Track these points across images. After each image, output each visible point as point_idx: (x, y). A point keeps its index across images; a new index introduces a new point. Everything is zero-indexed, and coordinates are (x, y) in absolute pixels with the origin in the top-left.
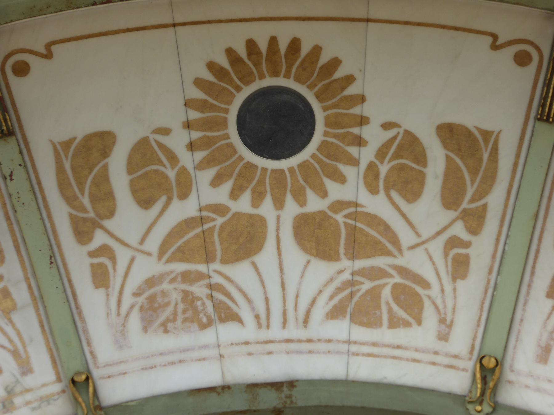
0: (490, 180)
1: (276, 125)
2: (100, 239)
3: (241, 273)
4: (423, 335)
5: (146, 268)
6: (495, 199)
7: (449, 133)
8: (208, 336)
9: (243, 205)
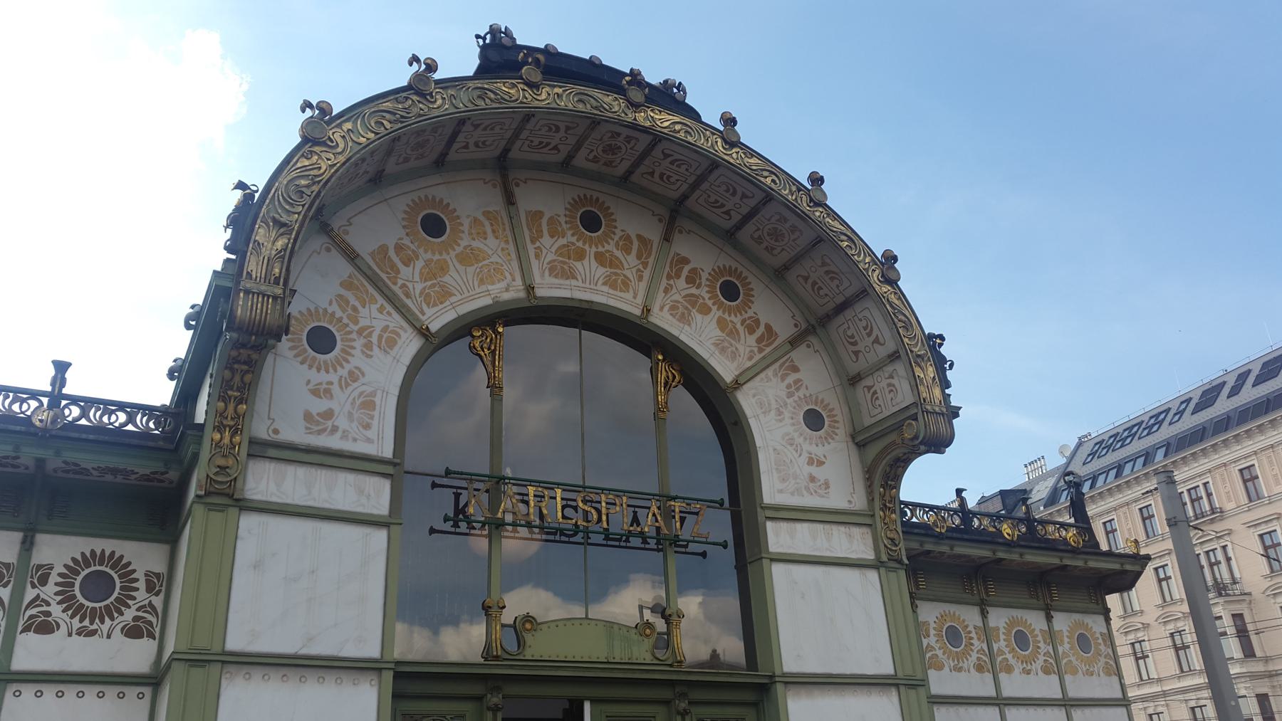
0: (649, 254)
2: (538, 244)
3: (578, 265)
4: (629, 296)
6: (651, 260)
7: (639, 237)
8: (568, 282)
9: (580, 244)
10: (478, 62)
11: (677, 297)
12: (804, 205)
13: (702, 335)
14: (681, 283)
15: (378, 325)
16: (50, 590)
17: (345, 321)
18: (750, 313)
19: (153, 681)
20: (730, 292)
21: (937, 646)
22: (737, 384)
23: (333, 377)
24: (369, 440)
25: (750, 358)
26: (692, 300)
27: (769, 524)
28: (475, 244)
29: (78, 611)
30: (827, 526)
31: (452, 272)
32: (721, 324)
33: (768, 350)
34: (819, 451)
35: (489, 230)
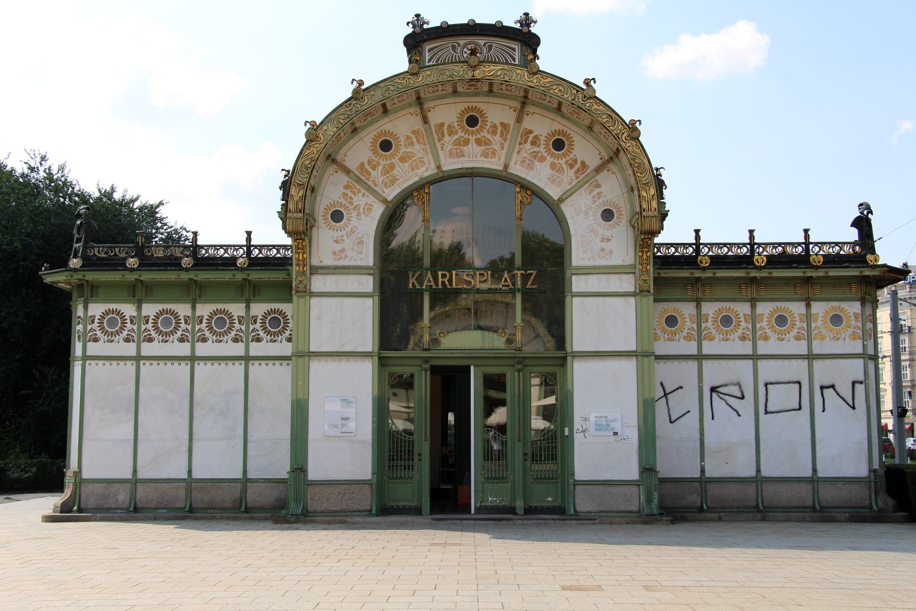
1: (472, 122)
3: (466, 148)
5: (450, 147)
6: (509, 136)
11: (525, 155)
13: (542, 175)
14: (528, 146)
15: (363, 203)
16: (258, 325)
17: (347, 205)
18: (572, 156)
20: (559, 145)
21: (711, 327)
22: (561, 200)
23: (344, 233)
24: (362, 259)
25: (570, 184)
26: (535, 155)
27: (574, 277)
28: (408, 150)
29: (269, 333)
30: (608, 276)
31: (397, 168)
32: (553, 166)
33: (582, 176)
35: (415, 140)
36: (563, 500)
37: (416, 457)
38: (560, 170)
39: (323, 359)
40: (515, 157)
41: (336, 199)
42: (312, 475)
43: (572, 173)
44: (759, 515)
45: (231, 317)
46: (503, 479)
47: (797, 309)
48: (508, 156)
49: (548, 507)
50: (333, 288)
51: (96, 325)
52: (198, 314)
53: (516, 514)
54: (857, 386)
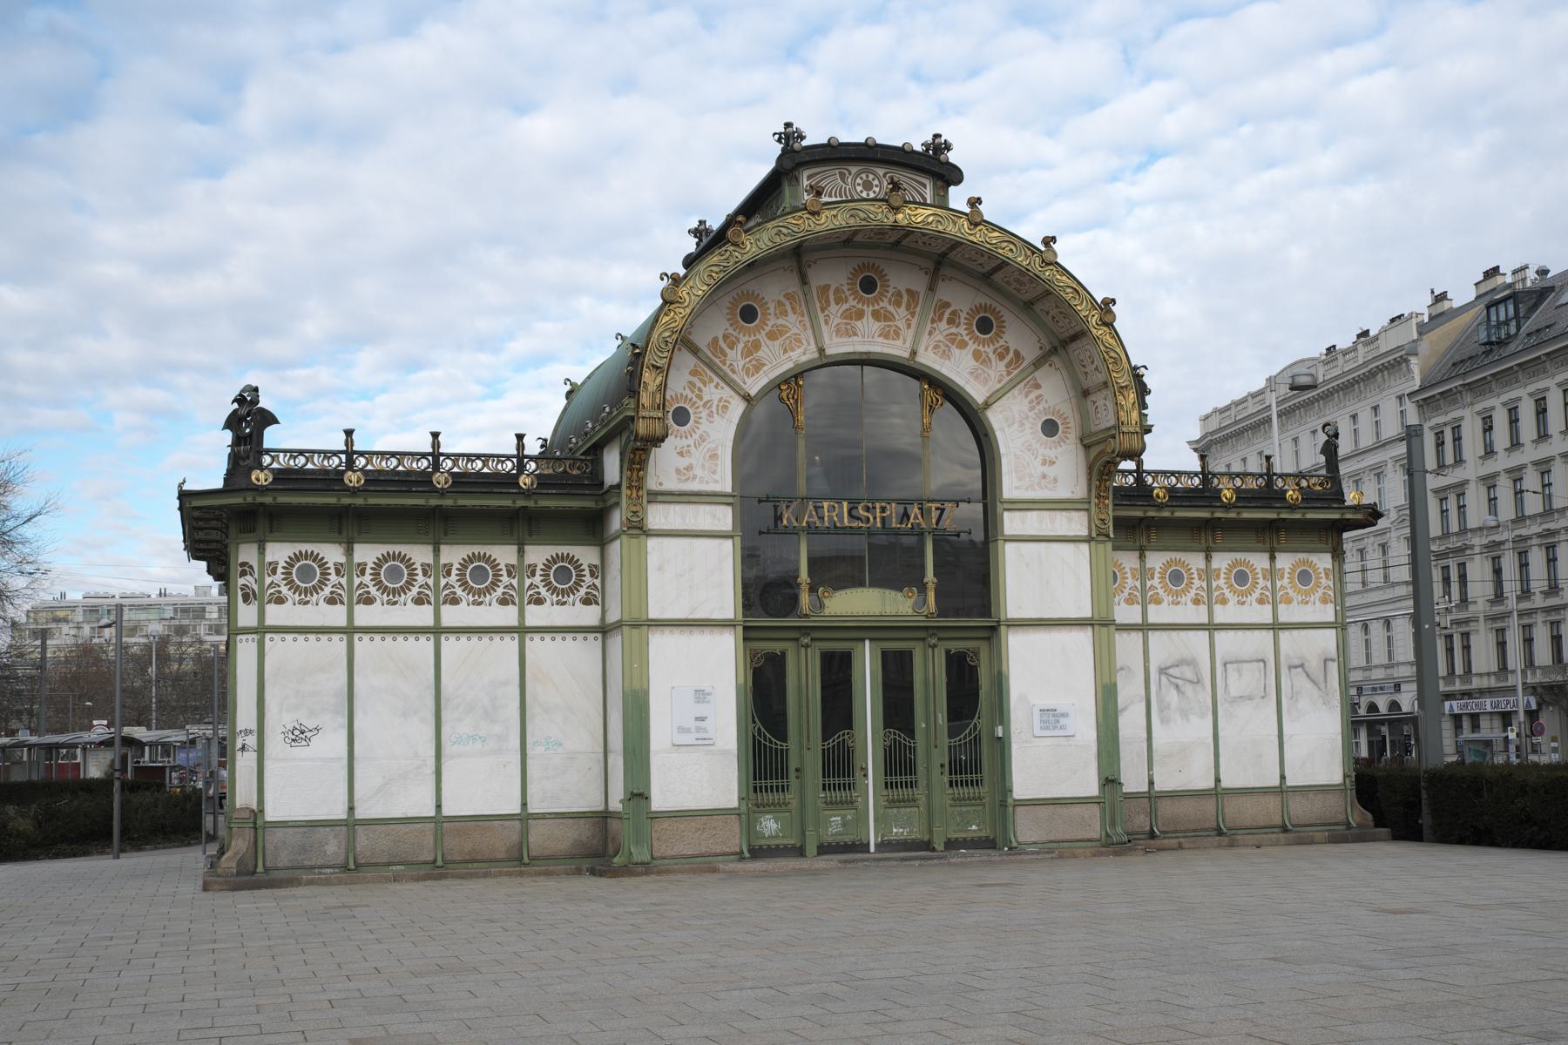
3: (859, 324)
4: (899, 343)
7: (909, 291)
10: (773, 165)
11: (940, 337)
12: (1035, 265)
13: (961, 368)
14: (943, 325)
15: (716, 398)
16: (537, 579)
18: (1002, 342)
19: (604, 630)
20: (984, 326)
22: (987, 405)
23: (690, 441)
24: (716, 481)
26: (952, 338)
31: (764, 348)
32: (977, 355)
34: (1051, 454)
36: (931, 832)
37: (792, 774)
38: (986, 361)
39: (667, 630)
40: (925, 339)
41: (680, 391)
42: (658, 802)
43: (1002, 366)
44: (1225, 840)
45: (495, 566)
46: (912, 802)
47: (1259, 561)
48: (916, 340)
49: (972, 839)
50: (677, 524)
51: (279, 576)
52: (443, 560)
53: (934, 850)
54: (1330, 664)
